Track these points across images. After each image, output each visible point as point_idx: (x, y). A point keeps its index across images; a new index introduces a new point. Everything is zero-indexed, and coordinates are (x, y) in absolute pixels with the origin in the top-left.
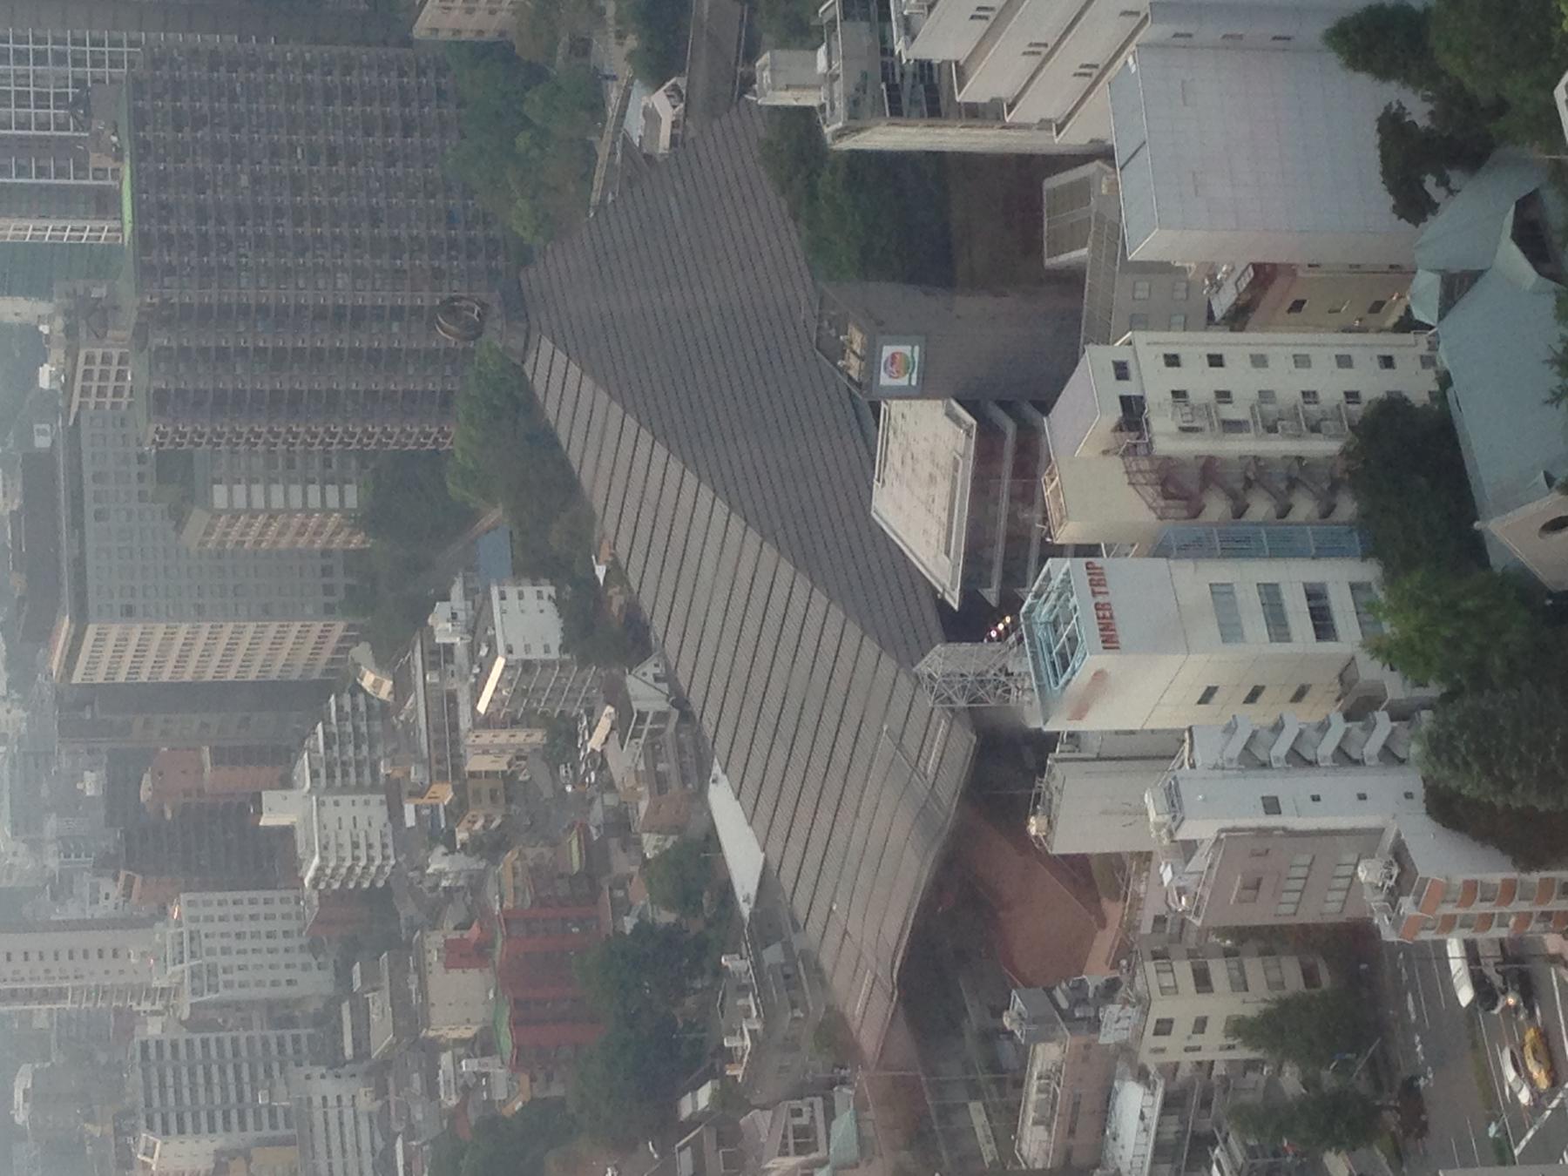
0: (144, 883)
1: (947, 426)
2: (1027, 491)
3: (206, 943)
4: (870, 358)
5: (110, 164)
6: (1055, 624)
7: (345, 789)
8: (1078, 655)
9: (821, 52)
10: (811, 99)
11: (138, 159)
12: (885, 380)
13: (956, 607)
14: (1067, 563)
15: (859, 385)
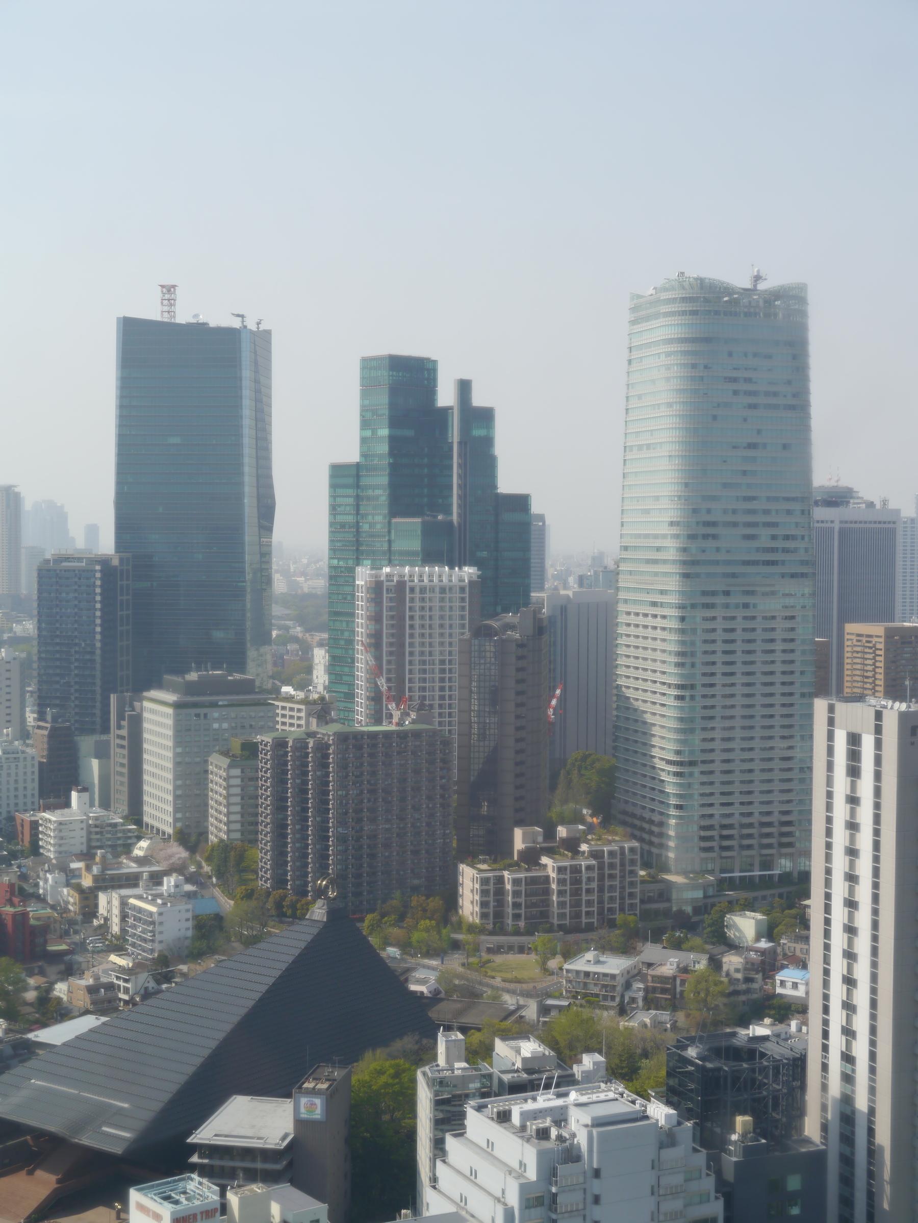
0: (43, 735)
1: (281, 1134)
2: (252, 1176)
3: (13, 765)
4: (313, 1092)
5: (395, 720)
6: (185, 1193)
7: (89, 833)
8: (171, 1205)
9: (464, 1065)
10: (441, 1060)
11: (398, 733)
12: (304, 1101)
13: (189, 1141)
14: (216, 1198)
15: (300, 1087)
